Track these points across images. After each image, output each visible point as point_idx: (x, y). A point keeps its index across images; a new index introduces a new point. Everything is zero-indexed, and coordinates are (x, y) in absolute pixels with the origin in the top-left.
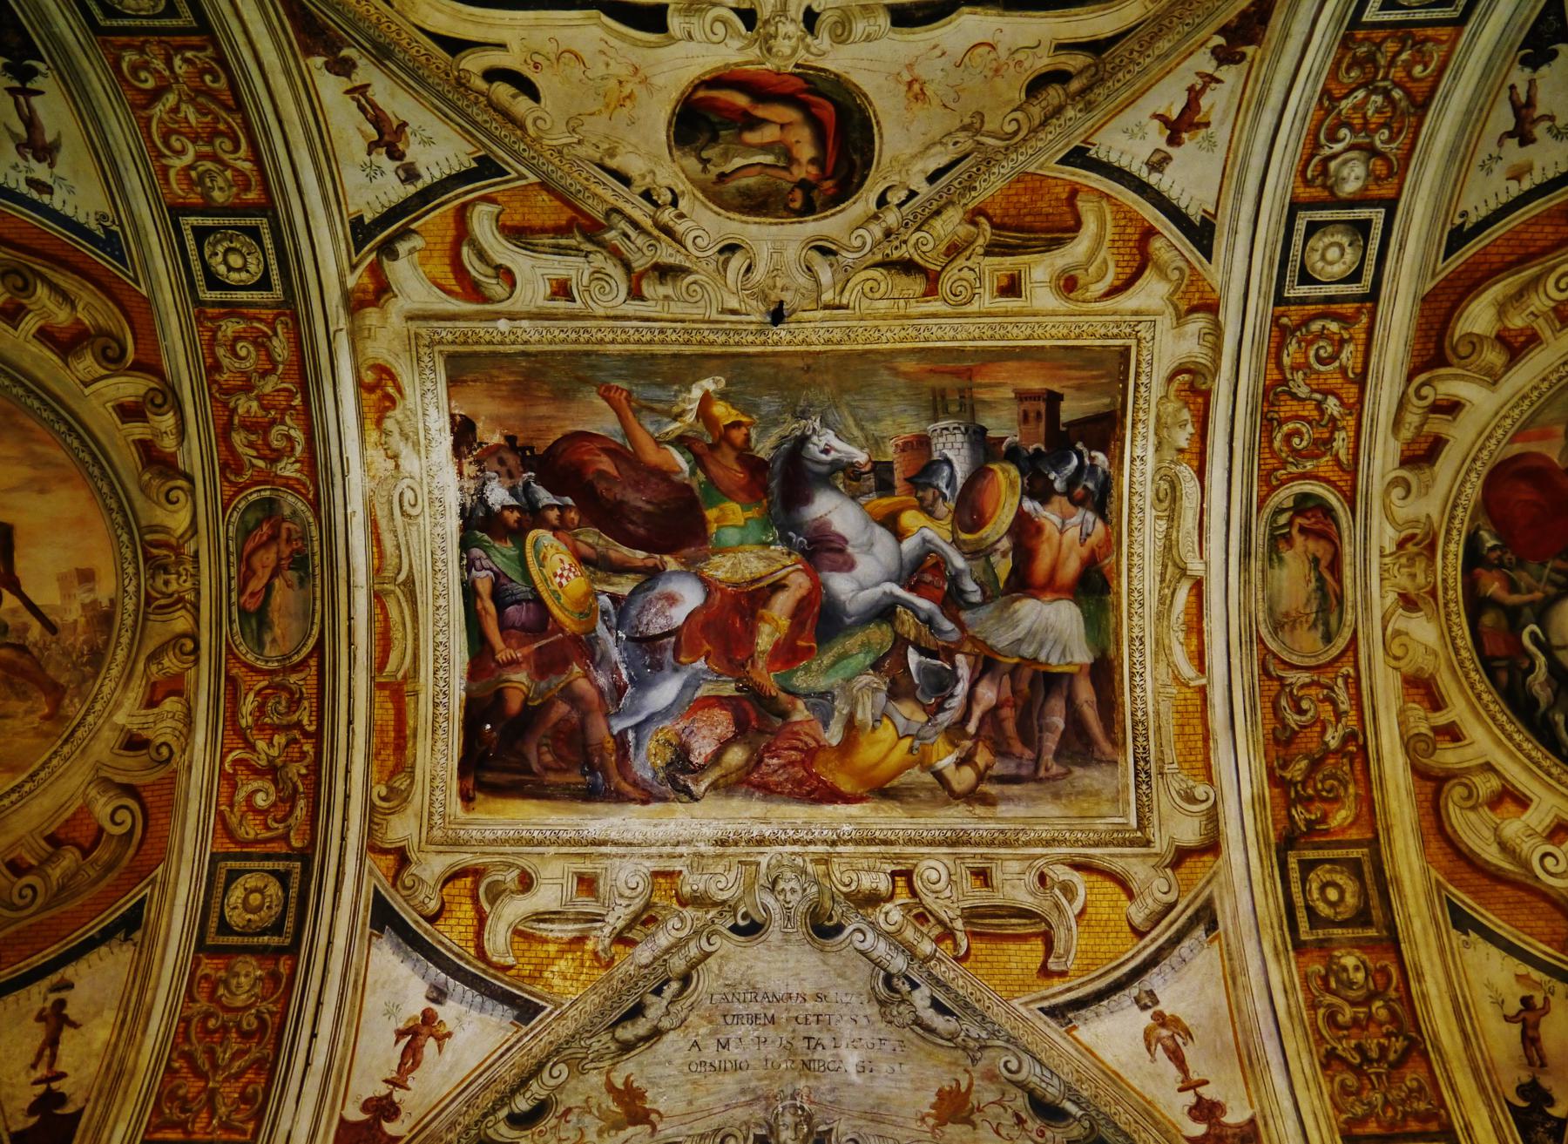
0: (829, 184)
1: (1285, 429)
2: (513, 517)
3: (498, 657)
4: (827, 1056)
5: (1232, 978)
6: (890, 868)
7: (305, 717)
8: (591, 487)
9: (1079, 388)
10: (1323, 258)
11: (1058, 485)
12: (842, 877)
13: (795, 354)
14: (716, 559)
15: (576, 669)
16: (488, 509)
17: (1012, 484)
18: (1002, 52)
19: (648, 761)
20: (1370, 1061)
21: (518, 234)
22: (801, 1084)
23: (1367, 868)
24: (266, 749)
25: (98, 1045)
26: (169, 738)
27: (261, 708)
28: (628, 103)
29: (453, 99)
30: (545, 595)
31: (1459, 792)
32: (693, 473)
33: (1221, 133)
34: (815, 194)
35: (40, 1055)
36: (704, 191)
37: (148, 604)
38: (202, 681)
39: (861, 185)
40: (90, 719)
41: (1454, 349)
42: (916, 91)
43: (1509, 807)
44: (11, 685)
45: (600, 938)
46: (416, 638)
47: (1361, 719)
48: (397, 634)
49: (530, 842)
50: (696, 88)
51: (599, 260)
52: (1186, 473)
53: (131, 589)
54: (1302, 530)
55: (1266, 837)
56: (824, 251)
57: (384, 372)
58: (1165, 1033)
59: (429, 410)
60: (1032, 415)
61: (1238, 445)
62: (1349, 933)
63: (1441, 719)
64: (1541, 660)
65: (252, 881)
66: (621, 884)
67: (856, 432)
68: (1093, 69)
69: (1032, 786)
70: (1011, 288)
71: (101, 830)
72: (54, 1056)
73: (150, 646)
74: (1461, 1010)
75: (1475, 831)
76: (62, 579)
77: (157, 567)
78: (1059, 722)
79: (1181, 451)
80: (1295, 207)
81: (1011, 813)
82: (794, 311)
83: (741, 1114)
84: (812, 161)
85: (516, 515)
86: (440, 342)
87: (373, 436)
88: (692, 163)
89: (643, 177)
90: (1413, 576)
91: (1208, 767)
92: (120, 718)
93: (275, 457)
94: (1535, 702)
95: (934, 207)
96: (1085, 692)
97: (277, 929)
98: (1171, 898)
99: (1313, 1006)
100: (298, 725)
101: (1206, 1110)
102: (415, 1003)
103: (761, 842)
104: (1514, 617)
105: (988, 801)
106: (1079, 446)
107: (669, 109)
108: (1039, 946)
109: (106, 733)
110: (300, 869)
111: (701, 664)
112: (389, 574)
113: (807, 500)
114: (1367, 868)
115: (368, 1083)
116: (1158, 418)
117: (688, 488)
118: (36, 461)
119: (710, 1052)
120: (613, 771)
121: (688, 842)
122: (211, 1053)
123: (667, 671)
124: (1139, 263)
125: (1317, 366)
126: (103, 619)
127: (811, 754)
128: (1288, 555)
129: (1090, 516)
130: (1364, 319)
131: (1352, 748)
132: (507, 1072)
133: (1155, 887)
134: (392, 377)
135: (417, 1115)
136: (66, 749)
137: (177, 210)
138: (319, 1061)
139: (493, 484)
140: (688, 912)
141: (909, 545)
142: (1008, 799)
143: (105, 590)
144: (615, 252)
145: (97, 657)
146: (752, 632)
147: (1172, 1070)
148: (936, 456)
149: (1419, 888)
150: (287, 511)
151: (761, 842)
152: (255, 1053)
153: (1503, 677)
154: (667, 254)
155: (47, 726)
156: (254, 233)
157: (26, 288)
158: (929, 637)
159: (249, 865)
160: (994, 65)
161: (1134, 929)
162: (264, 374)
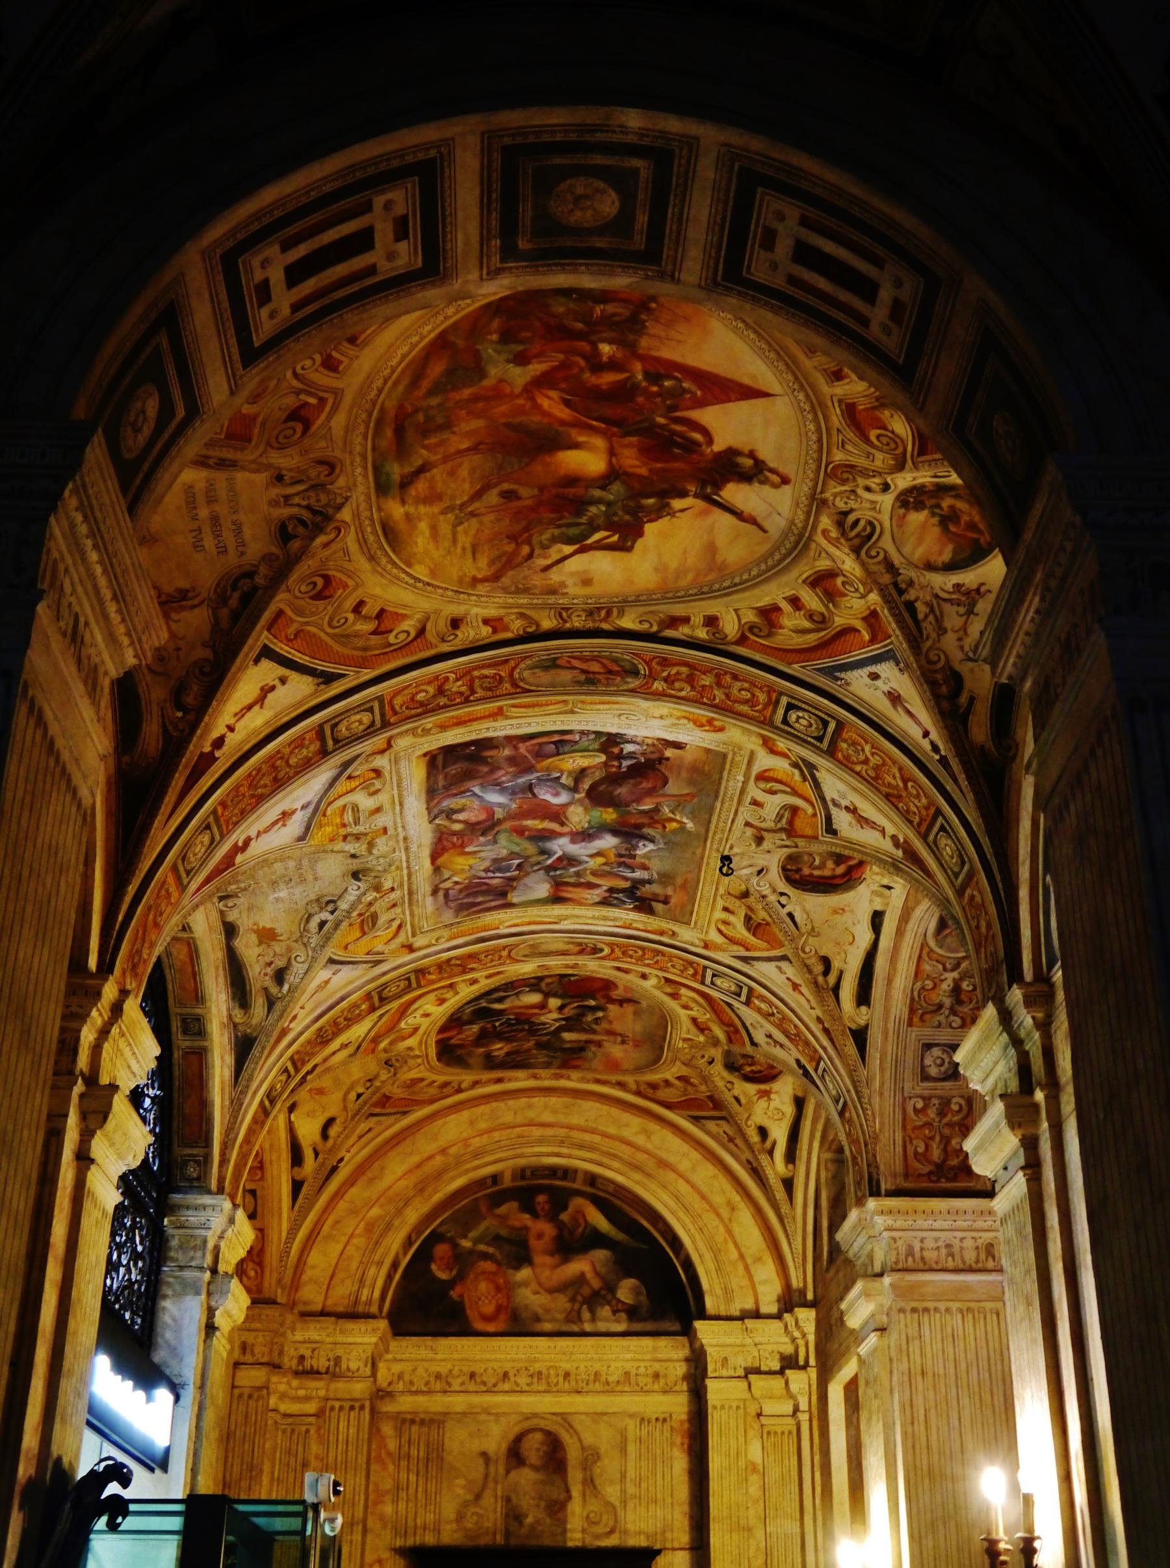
7: (480, 693)
18: (847, 947)
42: (839, 911)
44: (500, 557)
56: (760, 872)
70: (726, 909)
71: (390, 631)
73: (528, 612)
76: (585, 572)
77: (590, 613)
78: (480, 899)
80: (751, 990)
103: (407, 849)
118: (680, 573)
136: (450, 593)
140: (364, 847)
151: (407, 849)
157: (810, 616)
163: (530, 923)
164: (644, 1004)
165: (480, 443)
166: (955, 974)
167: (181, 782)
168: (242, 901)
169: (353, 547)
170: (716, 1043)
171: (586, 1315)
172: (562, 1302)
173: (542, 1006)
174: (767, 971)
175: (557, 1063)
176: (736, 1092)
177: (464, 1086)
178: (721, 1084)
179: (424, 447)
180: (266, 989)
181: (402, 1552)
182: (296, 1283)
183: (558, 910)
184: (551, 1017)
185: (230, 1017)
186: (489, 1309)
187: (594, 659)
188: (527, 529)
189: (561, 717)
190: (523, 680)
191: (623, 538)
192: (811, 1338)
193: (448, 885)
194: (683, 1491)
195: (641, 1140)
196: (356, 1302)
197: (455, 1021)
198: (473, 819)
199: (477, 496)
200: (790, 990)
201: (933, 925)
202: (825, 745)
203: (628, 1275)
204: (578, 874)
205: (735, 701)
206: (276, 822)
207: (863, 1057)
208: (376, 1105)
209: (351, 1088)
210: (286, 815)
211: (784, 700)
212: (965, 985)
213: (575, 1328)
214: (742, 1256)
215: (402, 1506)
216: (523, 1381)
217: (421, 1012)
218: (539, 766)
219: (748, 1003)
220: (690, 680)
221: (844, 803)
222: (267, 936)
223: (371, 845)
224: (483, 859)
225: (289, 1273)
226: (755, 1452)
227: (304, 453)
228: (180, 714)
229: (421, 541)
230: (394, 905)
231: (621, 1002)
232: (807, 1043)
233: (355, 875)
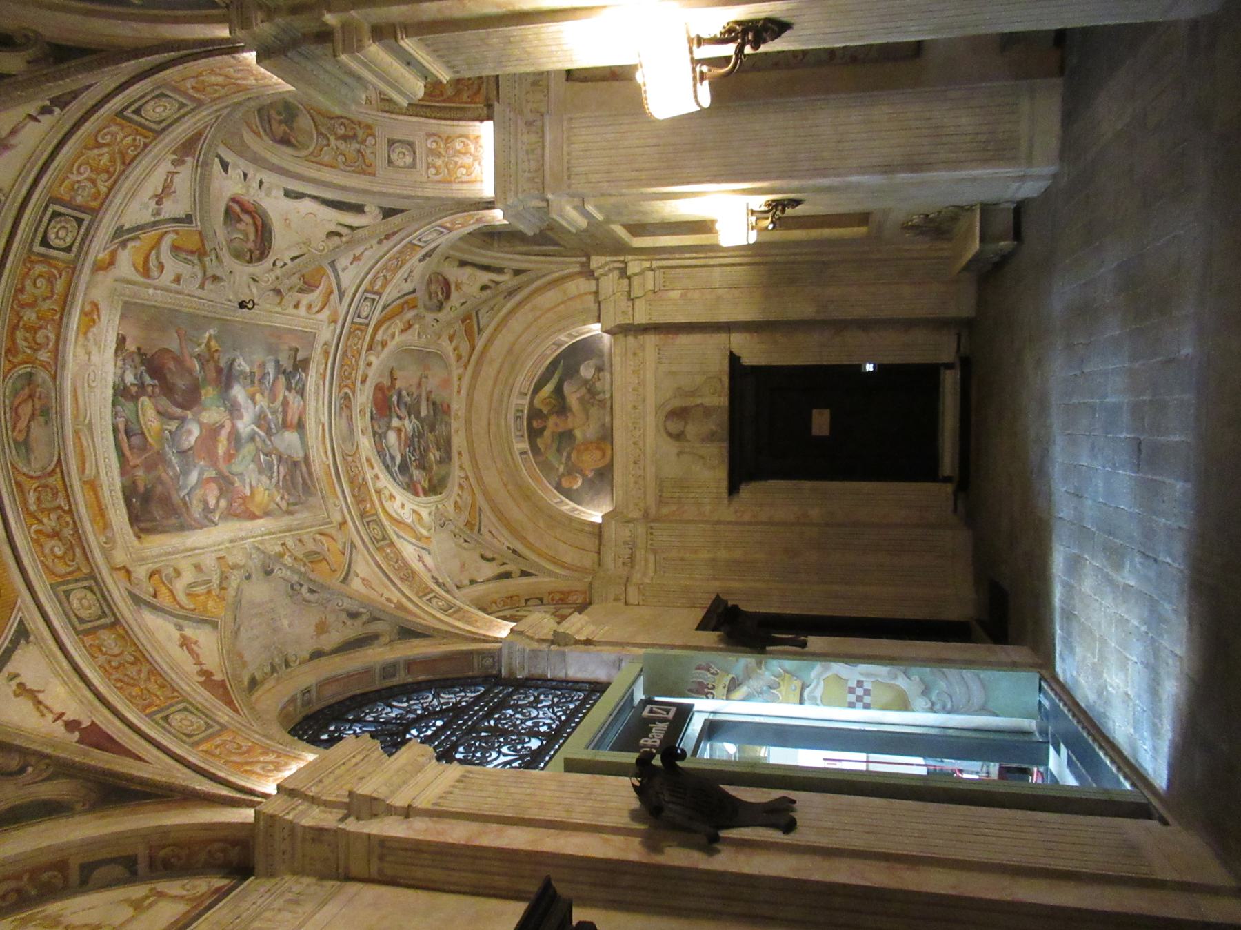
2: (134, 389)
3: (131, 464)
7: (62, 502)
19: (196, 510)
24: (50, 523)
27: (38, 499)
42: (287, 222)
48: (87, 453)
49: (169, 554)
56: (254, 280)
57: (95, 306)
59: (109, 328)
70: (296, 306)
72: (47, 708)
80: (366, 291)
86: (124, 295)
93: (37, 347)
100: (60, 507)
102: (177, 634)
112: (81, 419)
134: (98, 310)
139: (128, 372)
140: (236, 572)
141: (258, 407)
146: (216, 448)
150: (40, 380)
151: (243, 539)
162: (44, 299)
163: (324, 443)
164: (393, 364)
166: (332, 138)
167: (107, 756)
168: (291, 651)
170: (419, 317)
171: (601, 396)
172: (594, 411)
173: (399, 430)
174: (349, 278)
175: (446, 418)
176: (458, 305)
177: (462, 475)
178: (452, 314)
180: (364, 624)
181: (730, 501)
182: (583, 570)
183: (310, 424)
184: (409, 425)
185: (386, 645)
186: (598, 454)
187: (15, 410)
189: (97, 431)
190: (44, 469)
192: (608, 259)
193: (284, 505)
194: (697, 338)
195: (496, 366)
196: (593, 533)
197: (411, 488)
198: (216, 492)
200: (361, 263)
201: (289, 150)
202: (87, 218)
203: (578, 371)
204: (274, 413)
205: (52, 291)
206: (191, 651)
207: (402, 211)
208: (472, 529)
209: (461, 546)
210: (185, 643)
211: (38, 248)
212: (341, 131)
213: (608, 404)
214: (563, 303)
215: (706, 501)
216: (638, 433)
217: (400, 511)
218: (156, 447)
219: (380, 294)
220: (33, 330)
221: (153, 204)
222: (322, 628)
223: (235, 567)
224: (259, 481)
225: (576, 574)
226: (675, 294)
228: (30, 769)
230: (300, 541)
231: (393, 379)
232: (401, 252)
233: (268, 573)
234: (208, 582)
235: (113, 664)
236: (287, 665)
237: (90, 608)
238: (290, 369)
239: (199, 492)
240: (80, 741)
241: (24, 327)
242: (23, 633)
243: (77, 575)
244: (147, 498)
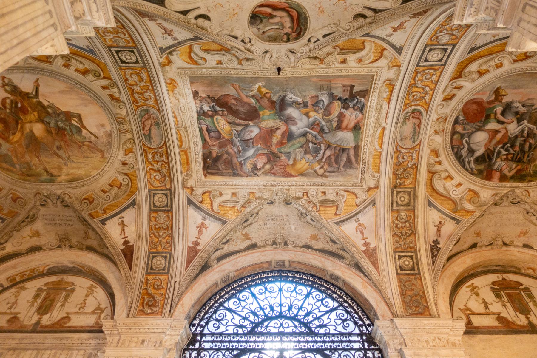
0: (294, 34)
1: (413, 94)
2: (210, 113)
4: (288, 226)
5: (377, 216)
6: (303, 191)
8: (230, 106)
9: (359, 84)
10: (432, 56)
11: (351, 106)
12: (292, 193)
13: (283, 77)
14: (262, 123)
15: (229, 147)
16: (204, 111)
17: (339, 106)
19: (247, 167)
20: (403, 235)
21: (207, 51)
22: (282, 231)
23: (412, 194)
24: (156, 166)
25: (133, 230)
26: (132, 162)
27: (153, 157)
28: (236, 15)
29: (187, 26)
30: (220, 130)
31: (438, 176)
32: (256, 104)
33: (409, 30)
34: (290, 37)
35: (121, 232)
36: (258, 37)
37: (120, 132)
38: (138, 149)
39: (303, 35)
40: (112, 158)
41: (464, 74)
42: (321, 10)
43: (449, 179)
45: (238, 206)
46: (189, 140)
47: (418, 160)
48: (184, 139)
49: (221, 185)
50: (256, 8)
51: (230, 57)
52: (385, 104)
53: (115, 128)
54: (413, 117)
55: (390, 186)
58: (360, 227)
59: (186, 89)
60: (346, 90)
61: (400, 98)
62: (404, 208)
63: (438, 159)
64: (466, 146)
65: (159, 196)
66: (242, 195)
67: (299, 94)
68: (373, 18)
69: (337, 173)
70: (344, 61)
71: (121, 183)
73: (123, 141)
74: (425, 224)
75: (439, 185)
76: (96, 126)
78: (344, 159)
79: (384, 98)
81: (332, 179)
82: (284, 68)
83: (269, 237)
84: (290, 27)
85: (211, 112)
87: (171, 94)
88: (255, 30)
89: (241, 36)
90: (439, 126)
91: (379, 169)
92: (119, 158)
93: (147, 100)
94: (461, 156)
95: (324, 45)
96: (352, 153)
97: (167, 206)
98: (366, 198)
99: (393, 223)
100: (163, 161)
101: (366, 244)
102: (200, 221)
103: (273, 186)
104: (462, 136)
105: (326, 176)
106: (358, 97)
107: (248, 15)
108: (335, 208)
109: (116, 161)
110: (169, 193)
111: (259, 146)
112: (180, 125)
113: (286, 109)
114: (412, 194)
115: (192, 238)
116: (380, 91)
117: (255, 107)
119: (263, 226)
120: (239, 170)
121: (257, 186)
122: (158, 233)
123: (251, 147)
124: (381, 54)
125: (425, 80)
126: (110, 135)
127: (285, 166)
128: (408, 123)
129: (358, 113)
130: (441, 70)
131: (414, 167)
132: (221, 236)
133: (362, 195)
134: (175, 81)
135: (204, 245)
136: (108, 165)
137: (109, 48)
138: (181, 234)
139: (204, 105)
140: (258, 201)
141: (311, 120)
142: (331, 176)
143: (108, 128)
144: (234, 55)
145: (110, 144)
146: (271, 139)
147: (361, 235)
148: (320, 99)
149: (423, 198)
150: (152, 112)
151: (273, 186)
152: (167, 233)
153: (456, 150)
154: (249, 55)
155: (102, 160)
156: (133, 52)
158: (315, 141)
159: (157, 192)
160: (345, 7)
161: (356, 205)
162: (140, 82)
165: (35, 155)
169: (75, 190)
179: (36, 169)
188: (76, 143)
191: (74, 116)
199: (59, 156)
222: (314, 237)
227: (30, 199)
229: (80, 172)
234: (237, 202)
235: (157, 227)
236: (286, 244)
237: (162, 202)
238: (346, 96)
239: (252, 160)
240: (122, 250)
241: (137, 93)
242: (133, 204)
243: (163, 188)
244: (217, 159)
